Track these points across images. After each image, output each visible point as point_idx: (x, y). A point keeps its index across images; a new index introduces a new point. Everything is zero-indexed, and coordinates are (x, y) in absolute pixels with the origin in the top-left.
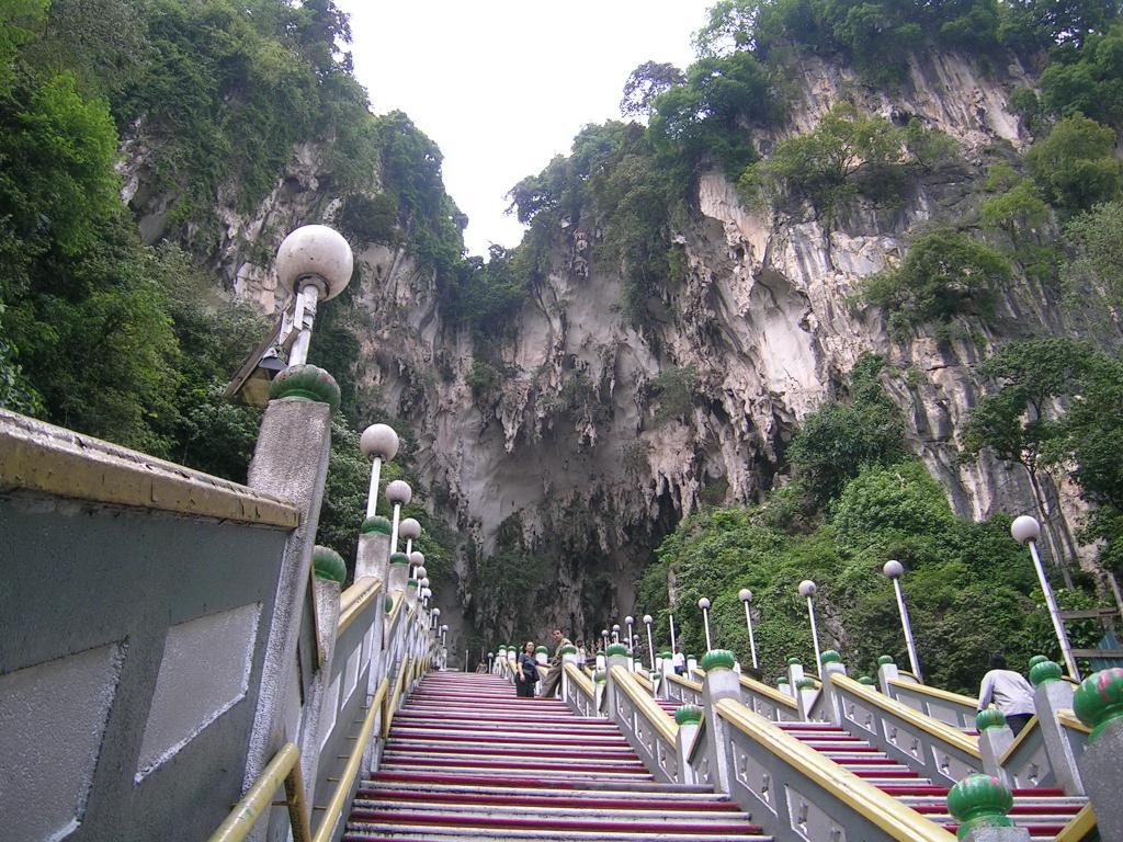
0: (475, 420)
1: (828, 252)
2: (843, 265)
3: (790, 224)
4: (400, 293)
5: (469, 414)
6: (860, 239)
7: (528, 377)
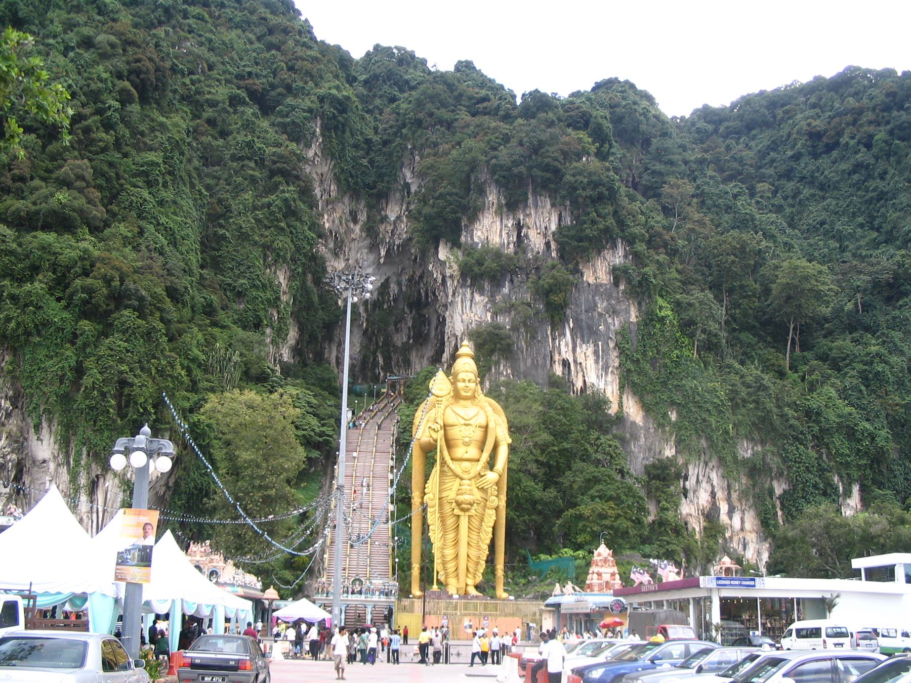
0: (367, 242)
1: (471, 301)
2: (474, 310)
3: (461, 287)
4: (332, 188)
5: (365, 239)
6: (482, 298)
7: (392, 219)
